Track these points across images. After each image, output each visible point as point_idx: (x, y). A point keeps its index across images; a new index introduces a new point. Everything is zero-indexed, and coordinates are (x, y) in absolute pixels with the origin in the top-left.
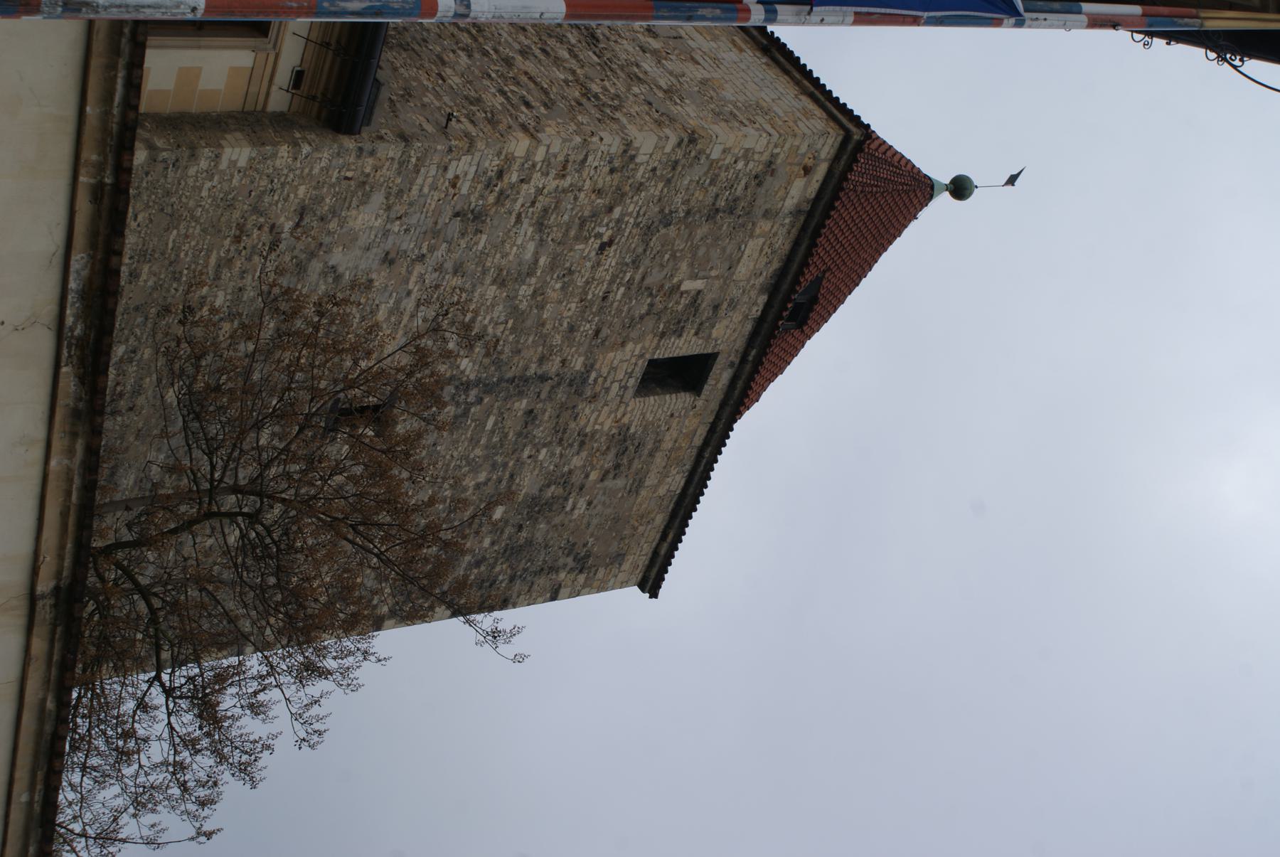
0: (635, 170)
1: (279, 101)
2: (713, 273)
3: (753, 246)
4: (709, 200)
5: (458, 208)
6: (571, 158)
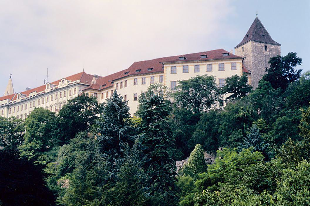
1: (250, 76)
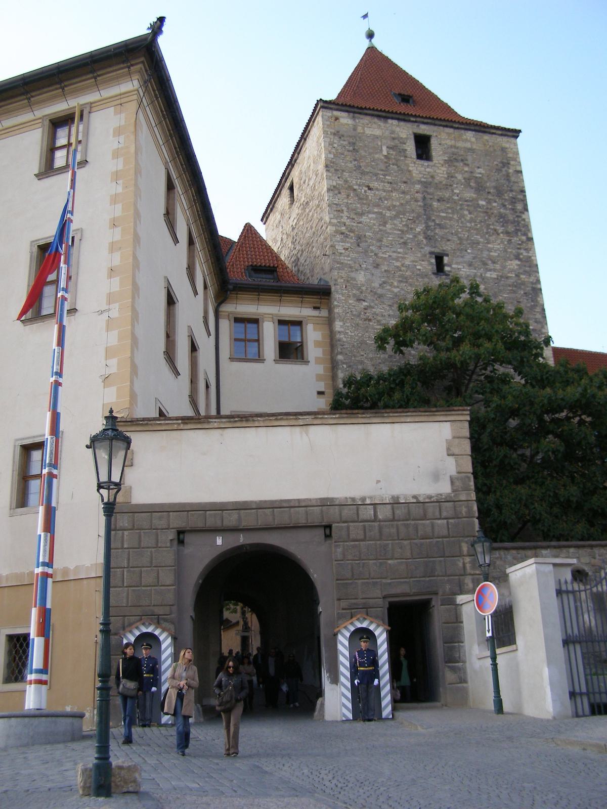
0: (339, 184)
1: (324, 313)
2: (380, 144)
3: (368, 131)
4: (350, 153)
5: (356, 245)
6: (335, 209)
